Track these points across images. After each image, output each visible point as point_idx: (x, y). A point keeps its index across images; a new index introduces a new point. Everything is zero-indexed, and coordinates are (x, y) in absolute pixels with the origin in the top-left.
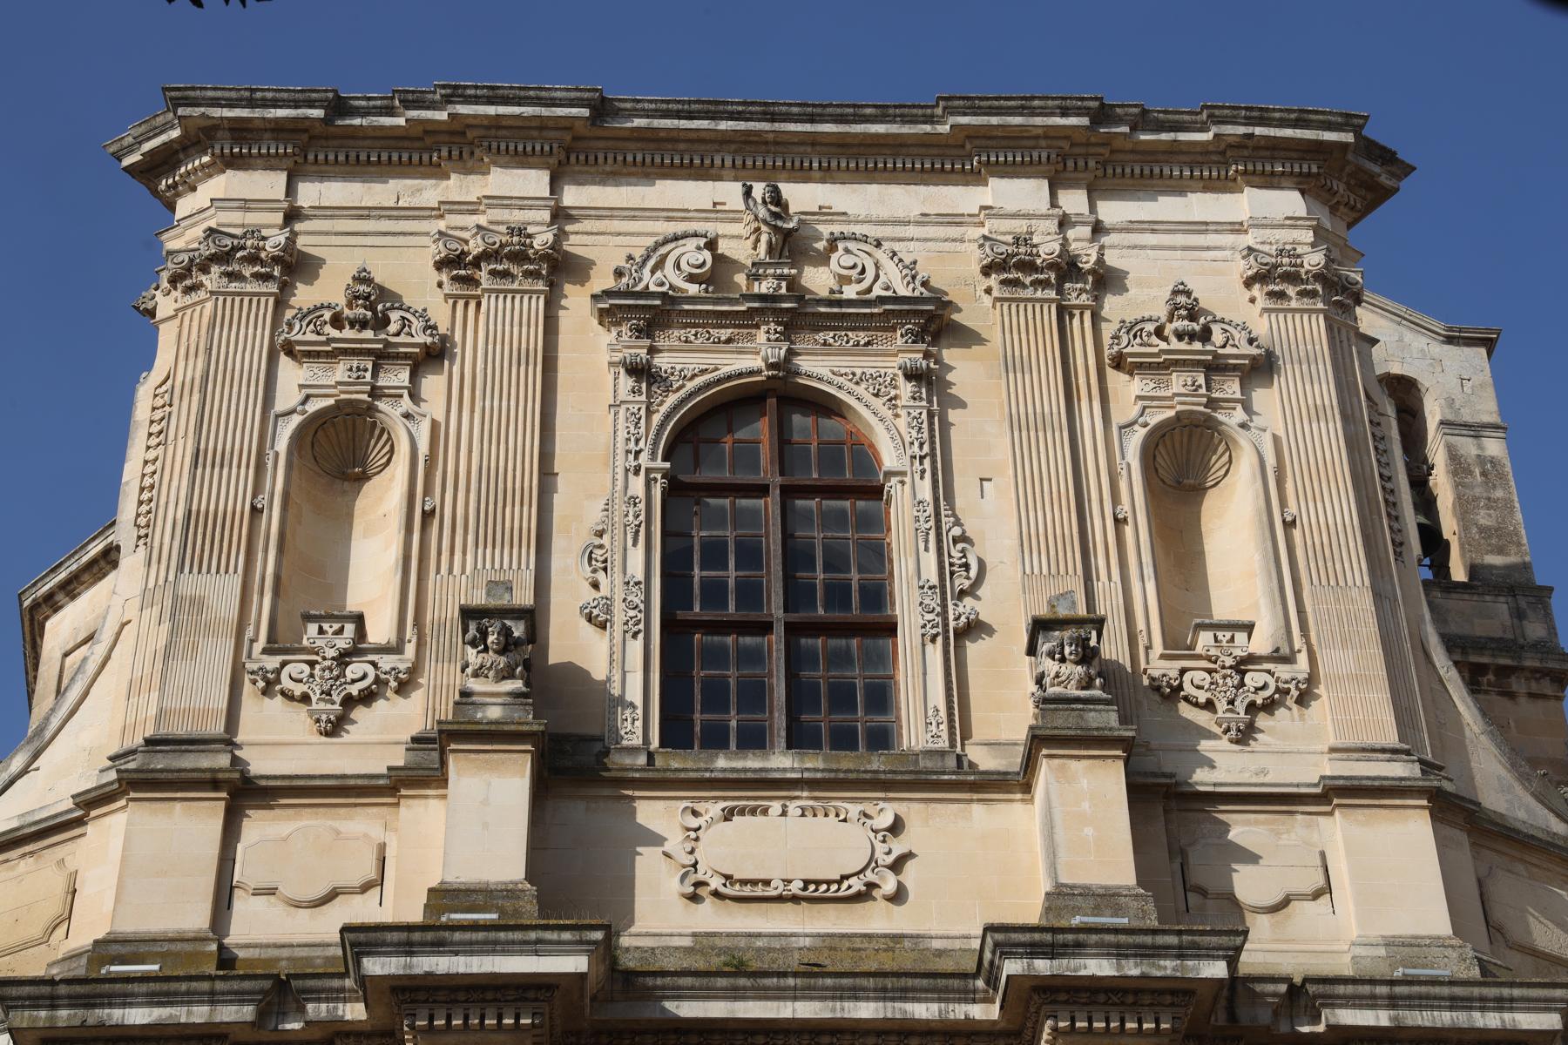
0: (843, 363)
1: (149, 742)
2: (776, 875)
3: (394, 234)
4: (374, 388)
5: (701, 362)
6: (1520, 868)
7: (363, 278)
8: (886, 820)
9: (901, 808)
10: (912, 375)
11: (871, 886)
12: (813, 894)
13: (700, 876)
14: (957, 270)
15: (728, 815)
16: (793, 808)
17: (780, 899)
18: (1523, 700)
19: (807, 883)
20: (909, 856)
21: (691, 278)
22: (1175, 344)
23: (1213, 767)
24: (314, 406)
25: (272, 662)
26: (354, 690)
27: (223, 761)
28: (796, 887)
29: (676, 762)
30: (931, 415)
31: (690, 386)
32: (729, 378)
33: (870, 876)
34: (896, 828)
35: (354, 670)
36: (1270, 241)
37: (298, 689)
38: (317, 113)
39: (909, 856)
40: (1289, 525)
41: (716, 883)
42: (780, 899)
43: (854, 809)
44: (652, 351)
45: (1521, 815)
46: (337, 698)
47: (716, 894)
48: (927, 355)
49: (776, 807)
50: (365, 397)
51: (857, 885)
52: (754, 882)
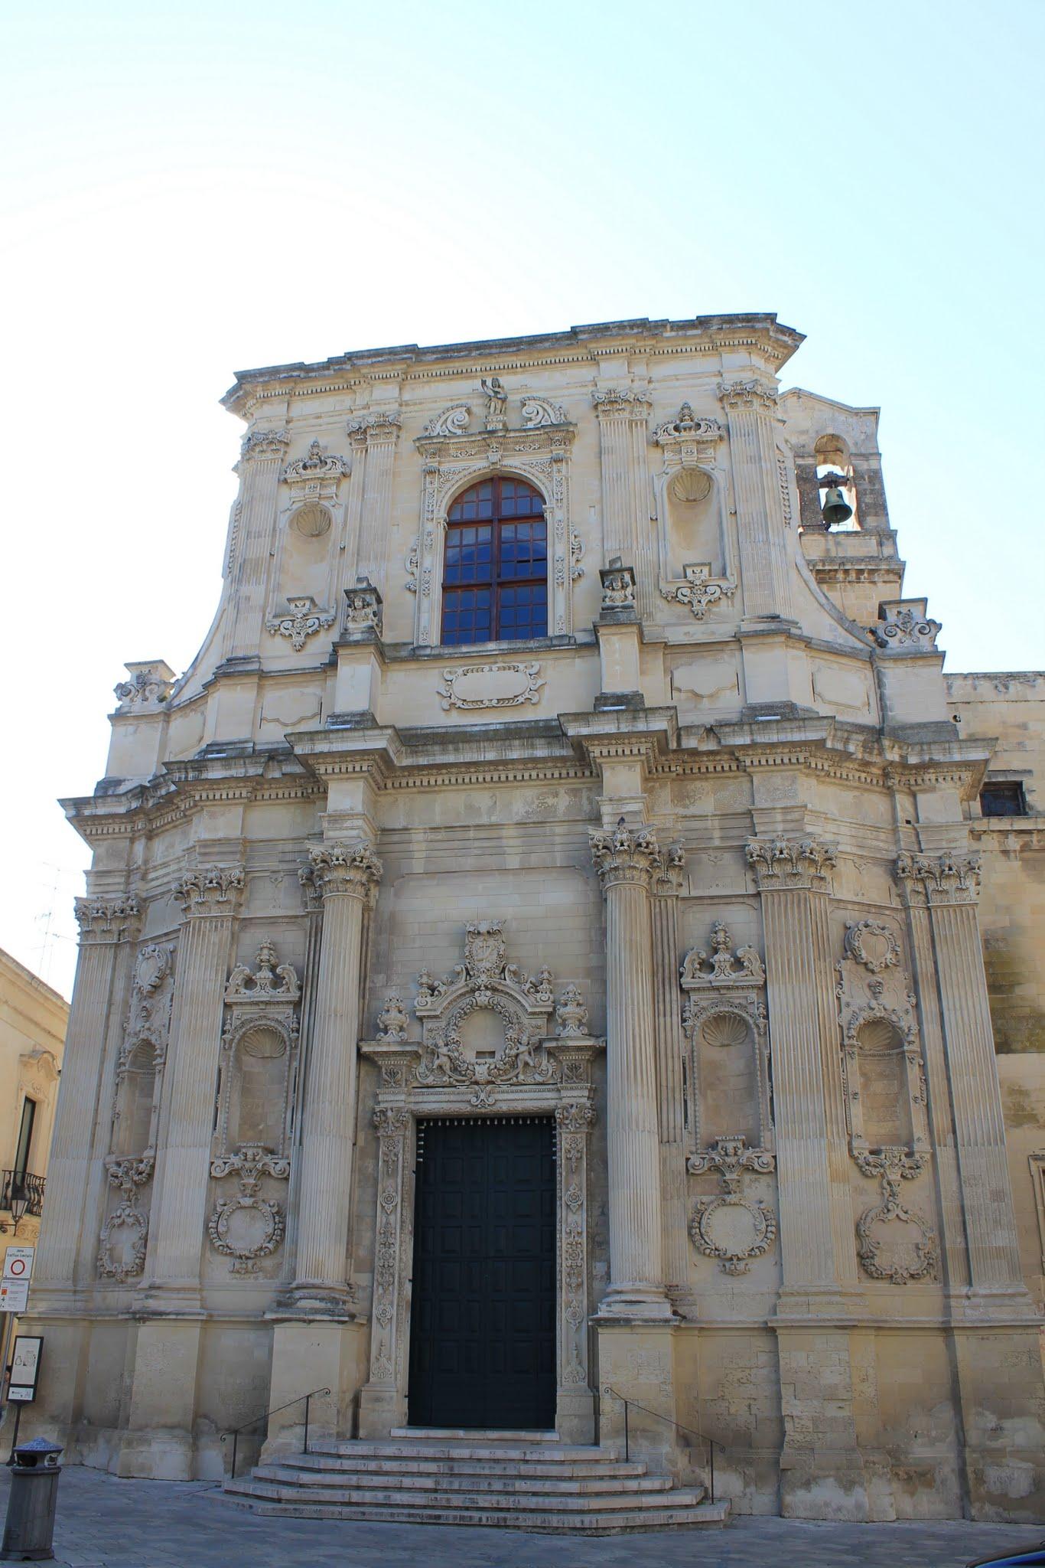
0: (526, 459)
1: (228, 660)
2: (485, 697)
6: (835, 666)
7: (315, 445)
8: (534, 670)
12: (503, 703)
14: (578, 409)
18: (880, 585)
23: (126, 665)
24: (295, 506)
25: (277, 622)
26: (310, 631)
27: (255, 666)
28: (494, 702)
29: (447, 651)
31: (457, 477)
35: (309, 623)
36: (730, 379)
37: (287, 633)
41: (459, 704)
45: (840, 641)
49: (487, 668)
51: (521, 699)
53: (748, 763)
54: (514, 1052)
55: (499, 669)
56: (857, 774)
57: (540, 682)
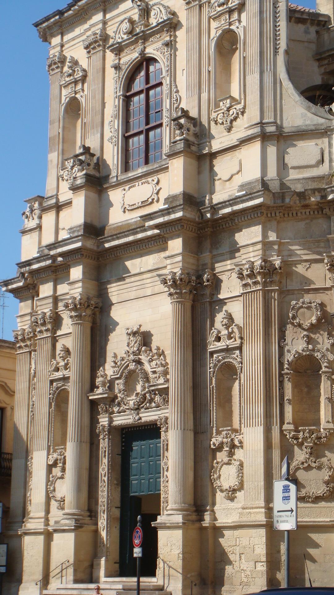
2: (136, 202)
3: (75, 45)
4: (75, 91)
5: (130, 56)
8: (156, 181)
9: (158, 176)
10: (167, 45)
11: (153, 199)
13: (125, 206)
15: (130, 188)
16: (140, 183)
17: (138, 208)
19: (142, 202)
20: (161, 189)
21: (124, 34)
22: (219, 9)
28: (140, 204)
30: (171, 55)
32: (135, 59)
33: (153, 197)
34: (158, 183)
38: (57, 17)
39: (161, 189)
40: (244, 58)
42: (138, 208)
43: (150, 180)
44: (120, 59)
45: (308, 122)
46: (72, 178)
47: (128, 210)
48: (171, 36)
49: (137, 183)
50: (73, 95)
51: (150, 200)
52: (133, 205)
53: (236, 221)
54: (143, 393)
55: (142, 184)
56: (304, 211)
57: (158, 188)
